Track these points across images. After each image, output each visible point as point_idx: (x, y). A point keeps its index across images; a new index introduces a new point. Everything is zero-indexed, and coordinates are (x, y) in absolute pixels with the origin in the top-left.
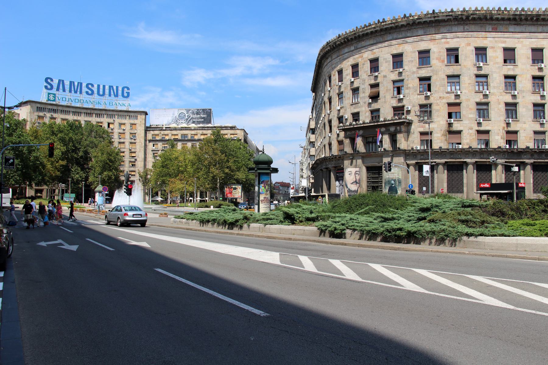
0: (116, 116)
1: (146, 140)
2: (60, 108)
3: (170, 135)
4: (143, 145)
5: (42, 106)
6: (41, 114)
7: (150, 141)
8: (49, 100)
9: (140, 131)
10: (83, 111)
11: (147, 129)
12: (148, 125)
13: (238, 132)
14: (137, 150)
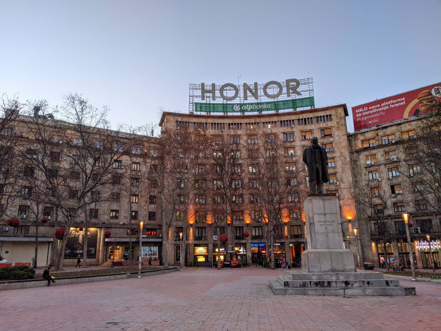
1: (351, 153)
3: (398, 134)
4: (348, 159)
7: (359, 152)
14: (339, 170)
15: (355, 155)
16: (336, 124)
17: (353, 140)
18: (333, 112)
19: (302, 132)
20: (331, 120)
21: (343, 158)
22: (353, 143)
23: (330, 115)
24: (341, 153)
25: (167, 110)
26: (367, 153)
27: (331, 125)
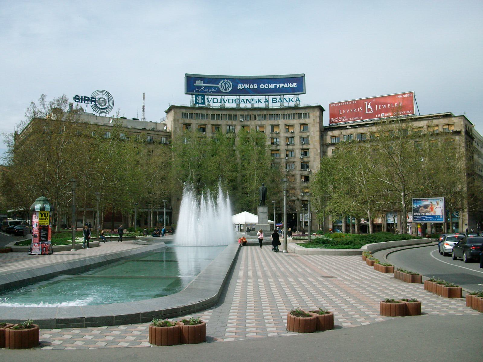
0: (282, 117)
2: (210, 112)
4: (319, 151)
5: (189, 111)
6: (187, 121)
8: (196, 103)
9: (314, 133)
10: (239, 113)
11: (324, 131)
12: (326, 123)
13: (454, 120)
15: (325, 147)
16: (312, 121)
17: (324, 135)
19: (286, 125)
20: (309, 117)
21: (315, 150)
22: (325, 137)
23: (309, 113)
24: (314, 145)
25: (174, 104)
26: (333, 147)
27: (309, 122)
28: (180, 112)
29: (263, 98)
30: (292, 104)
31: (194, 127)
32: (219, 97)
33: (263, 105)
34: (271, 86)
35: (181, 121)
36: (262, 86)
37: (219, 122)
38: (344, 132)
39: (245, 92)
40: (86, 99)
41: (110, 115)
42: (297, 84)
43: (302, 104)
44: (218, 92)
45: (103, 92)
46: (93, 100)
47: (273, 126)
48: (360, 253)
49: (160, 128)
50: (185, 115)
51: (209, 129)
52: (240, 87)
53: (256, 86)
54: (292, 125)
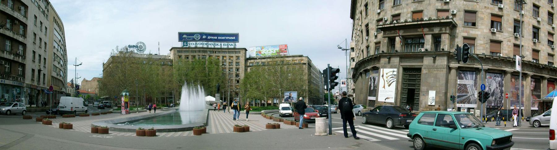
2: (190, 50)
5: (180, 50)
6: (180, 54)
10: (208, 50)
11: (247, 60)
12: (248, 57)
13: (304, 58)
18: (241, 51)
28: (176, 50)
29: (219, 43)
30: (232, 47)
31: (183, 57)
32: (194, 42)
33: (219, 47)
34: (223, 38)
35: (177, 54)
36: (219, 38)
37: (195, 54)
38: (256, 61)
39: (211, 40)
40: (133, 46)
41: (145, 53)
42: (235, 37)
43: (237, 47)
44: (194, 40)
45: (141, 42)
46: (136, 47)
47: (223, 57)
48: (261, 114)
49: (167, 58)
50: (179, 52)
51: (190, 57)
52: (209, 38)
53: (216, 38)
54: (232, 57)
